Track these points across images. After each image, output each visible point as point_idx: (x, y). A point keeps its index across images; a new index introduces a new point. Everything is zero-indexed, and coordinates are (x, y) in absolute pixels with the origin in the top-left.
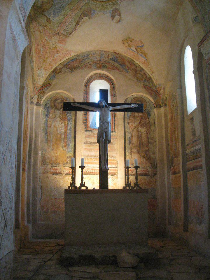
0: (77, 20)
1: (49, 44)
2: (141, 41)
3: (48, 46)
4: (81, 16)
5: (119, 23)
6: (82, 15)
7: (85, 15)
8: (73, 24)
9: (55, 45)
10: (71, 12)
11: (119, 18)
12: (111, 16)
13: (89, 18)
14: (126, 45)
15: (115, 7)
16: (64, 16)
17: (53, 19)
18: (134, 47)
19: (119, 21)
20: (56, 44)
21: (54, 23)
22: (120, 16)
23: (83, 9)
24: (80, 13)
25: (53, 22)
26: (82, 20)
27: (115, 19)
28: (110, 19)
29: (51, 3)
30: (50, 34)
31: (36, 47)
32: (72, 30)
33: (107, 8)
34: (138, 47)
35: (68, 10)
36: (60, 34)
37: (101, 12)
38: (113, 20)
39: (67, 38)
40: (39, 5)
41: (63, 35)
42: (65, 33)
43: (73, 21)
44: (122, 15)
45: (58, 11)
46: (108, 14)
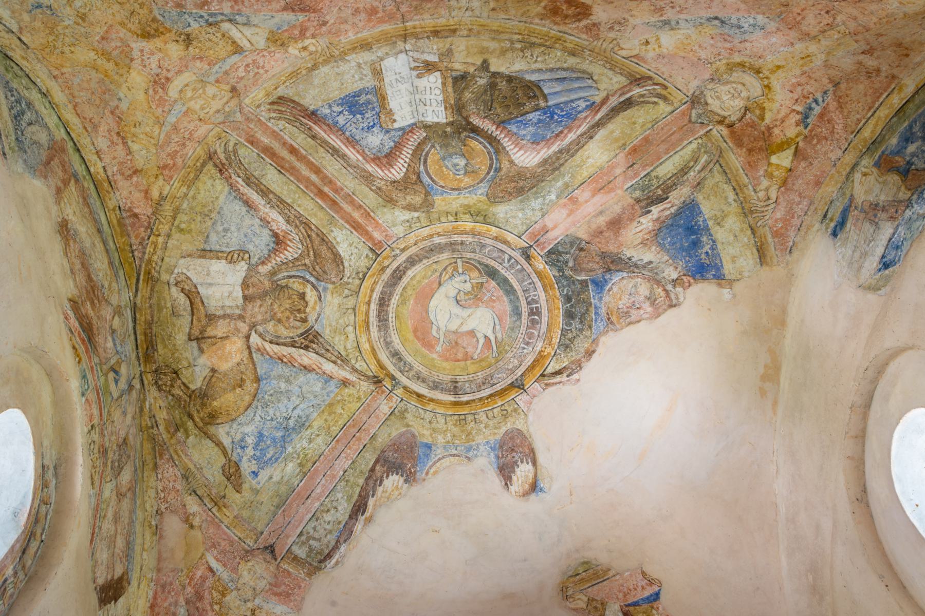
0: (358, 490)
1: (224, 595)
2: (644, 574)
3: (216, 607)
4: (372, 470)
5: (533, 496)
6: (378, 468)
7: (394, 467)
8: (340, 508)
9: (250, 605)
10: (333, 449)
11: (531, 475)
12: (495, 466)
13: (406, 481)
14: (582, 605)
15: (509, 426)
16: (300, 465)
17: (255, 474)
18: (617, 607)
19: (534, 487)
20: (257, 601)
21: (256, 492)
22: (534, 463)
23: (383, 439)
24: (370, 458)
25: (252, 489)
26: (380, 490)
27: (514, 478)
28: (495, 481)
29: (250, 386)
30: (232, 543)
31: (155, 598)
32: (332, 538)
33: (479, 430)
34: (635, 604)
35: (319, 440)
36: (280, 551)
37: (454, 452)
38: (506, 484)
39: (310, 574)
40: (199, 385)
41: (296, 558)
42: (301, 552)
43: (339, 495)
44: (541, 458)
45: (279, 434)
46: (485, 462)
